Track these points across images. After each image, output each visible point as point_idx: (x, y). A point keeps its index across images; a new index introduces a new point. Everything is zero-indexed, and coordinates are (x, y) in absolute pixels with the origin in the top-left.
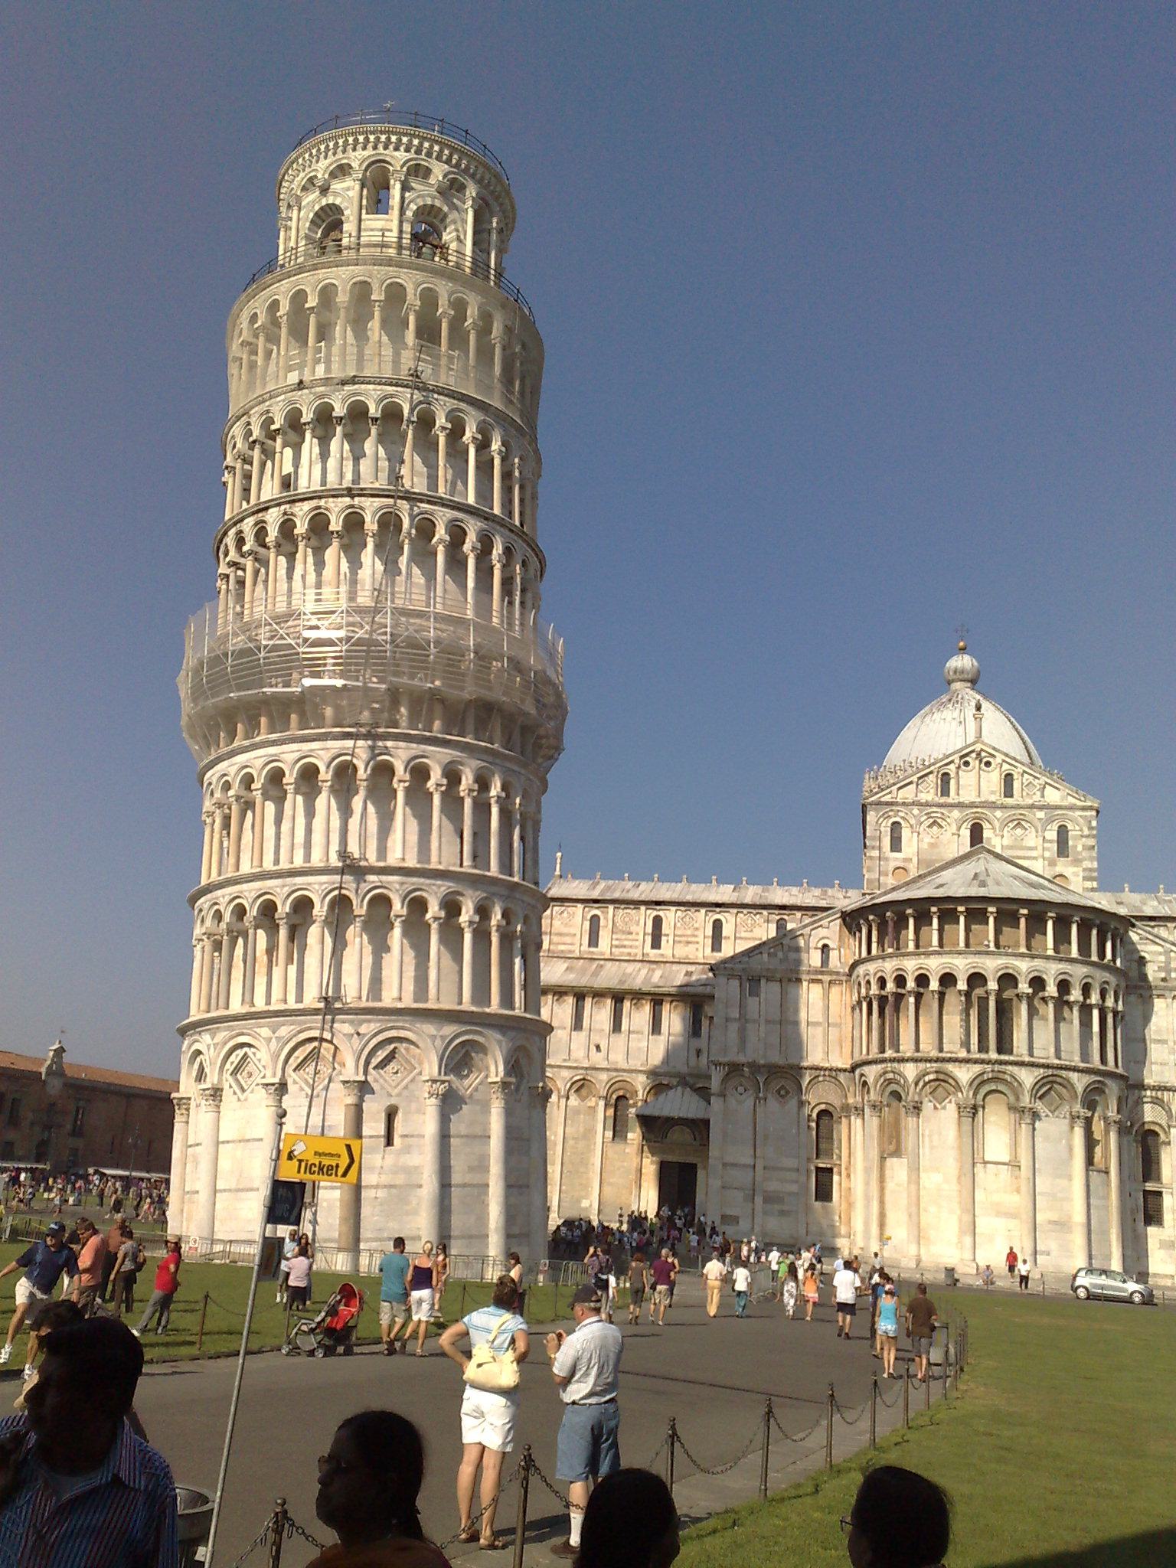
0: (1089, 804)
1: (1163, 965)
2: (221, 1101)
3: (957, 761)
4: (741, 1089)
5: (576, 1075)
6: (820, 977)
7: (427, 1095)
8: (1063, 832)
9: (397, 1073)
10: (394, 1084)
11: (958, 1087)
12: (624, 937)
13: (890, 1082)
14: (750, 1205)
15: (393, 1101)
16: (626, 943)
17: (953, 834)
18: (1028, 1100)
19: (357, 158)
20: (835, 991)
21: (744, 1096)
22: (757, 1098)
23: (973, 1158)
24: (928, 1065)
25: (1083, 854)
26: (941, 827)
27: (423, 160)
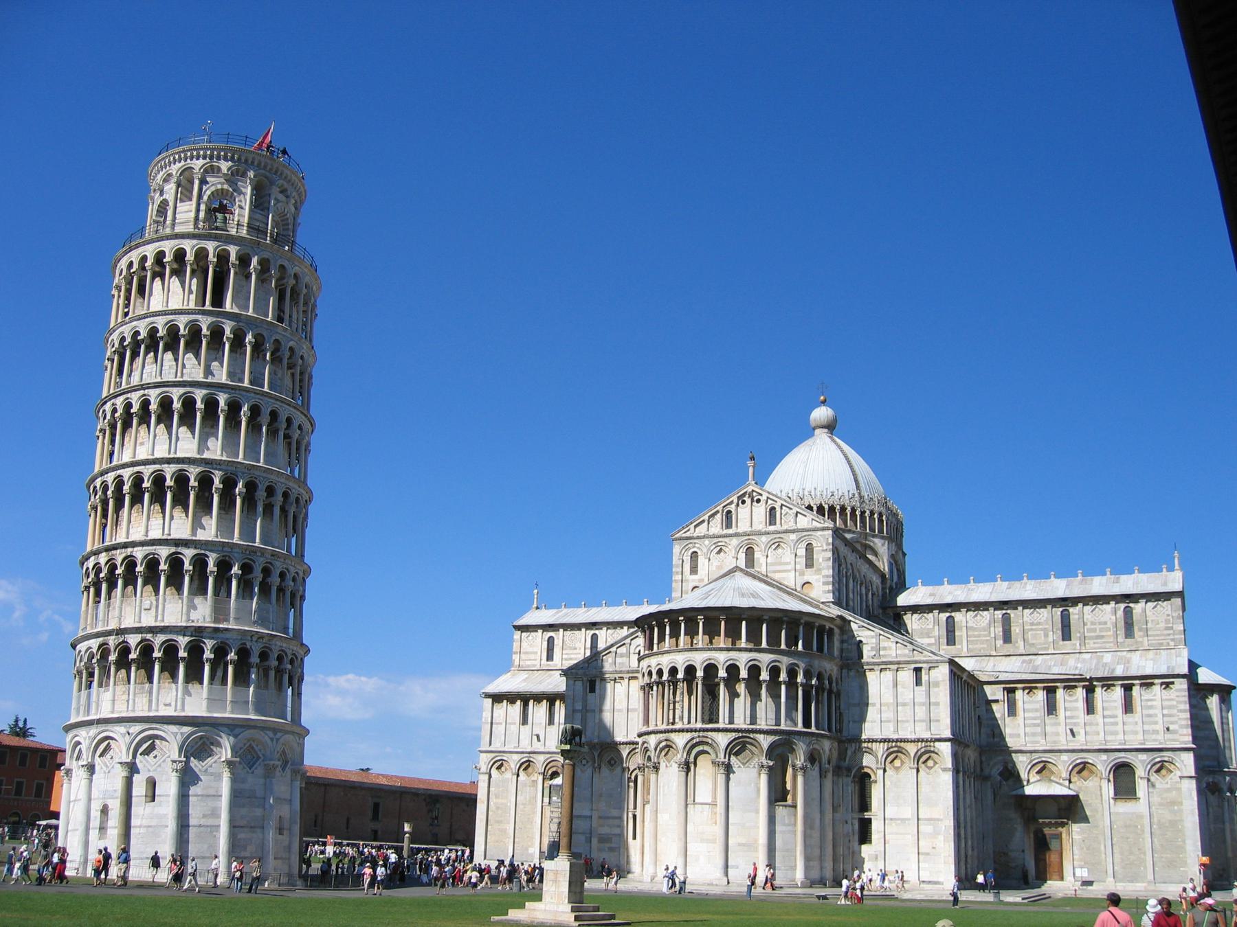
0: (826, 525)
1: (874, 645)
3: (736, 501)
4: (584, 762)
5: (523, 758)
8: (809, 549)
11: (677, 751)
12: (571, 652)
14: (589, 844)
16: (573, 656)
18: (722, 756)
19: (175, 169)
21: (585, 768)
23: (688, 799)
24: (661, 735)
25: (823, 565)
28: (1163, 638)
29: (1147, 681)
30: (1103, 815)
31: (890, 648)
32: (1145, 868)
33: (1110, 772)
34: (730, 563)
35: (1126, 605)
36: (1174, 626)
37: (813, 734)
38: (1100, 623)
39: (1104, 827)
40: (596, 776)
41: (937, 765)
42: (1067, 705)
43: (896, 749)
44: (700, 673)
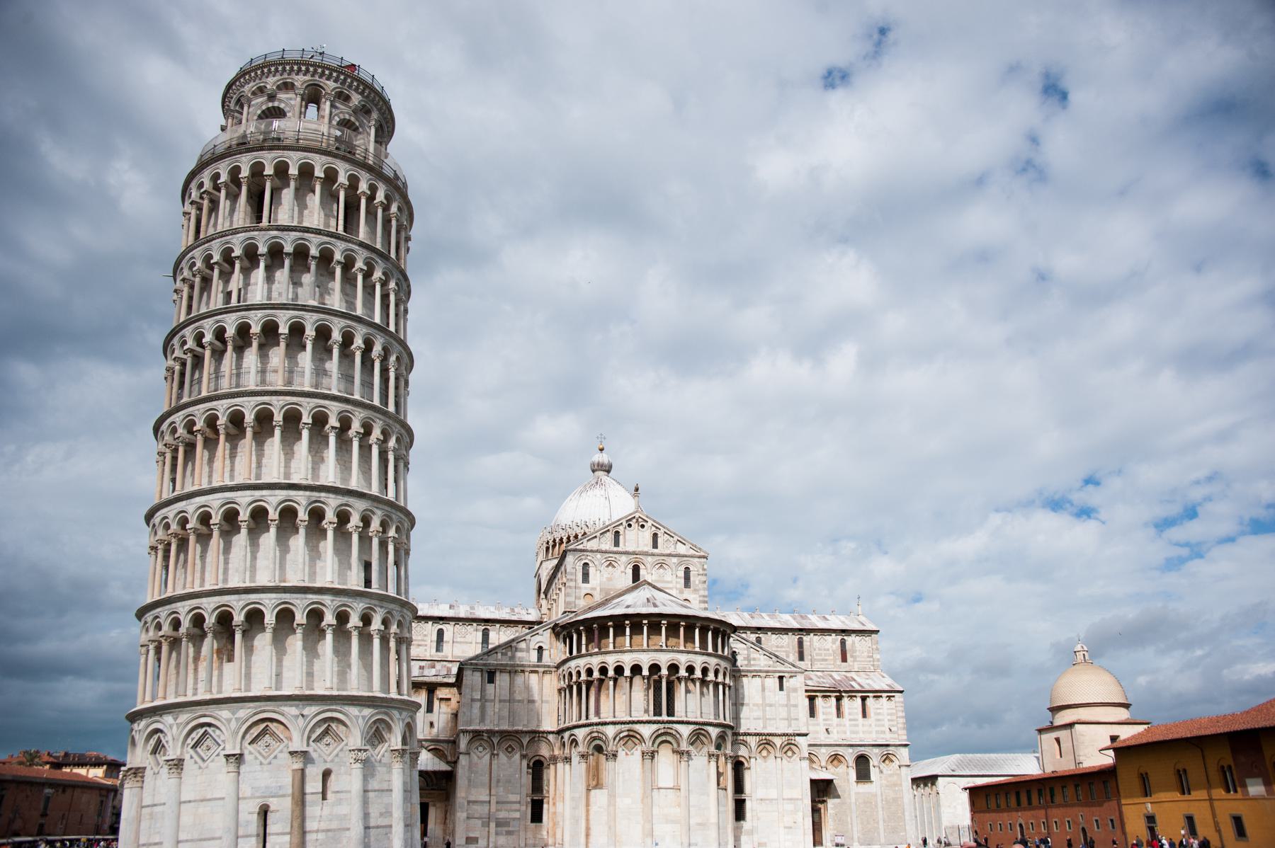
2: (182, 769)
3: (624, 524)
4: (481, 749)
6: (537, 669)
7: (352, 761)
8: (687, 570)
9: (329, 744)
10: (328, 753)
11: (642, 740)
13: (595, 739)
15: (328, 766)
17: (622, 572)
20: (547, 677)
22: (493, 754)
23: (652, 786)
24: (623, 726)
25: (700, 586)
26: (614, 567)
27: (346, 89)
29: (877, 694)
30: (850, 794)
31: (759, 659)
32: (878, 833)
35: (842, 637)
38: (825, 650)
39: (850, 803)
40: (495, 762)
41: (796, 755)
42: (825, 710)
43: (765, 742)
44: (664, 672)
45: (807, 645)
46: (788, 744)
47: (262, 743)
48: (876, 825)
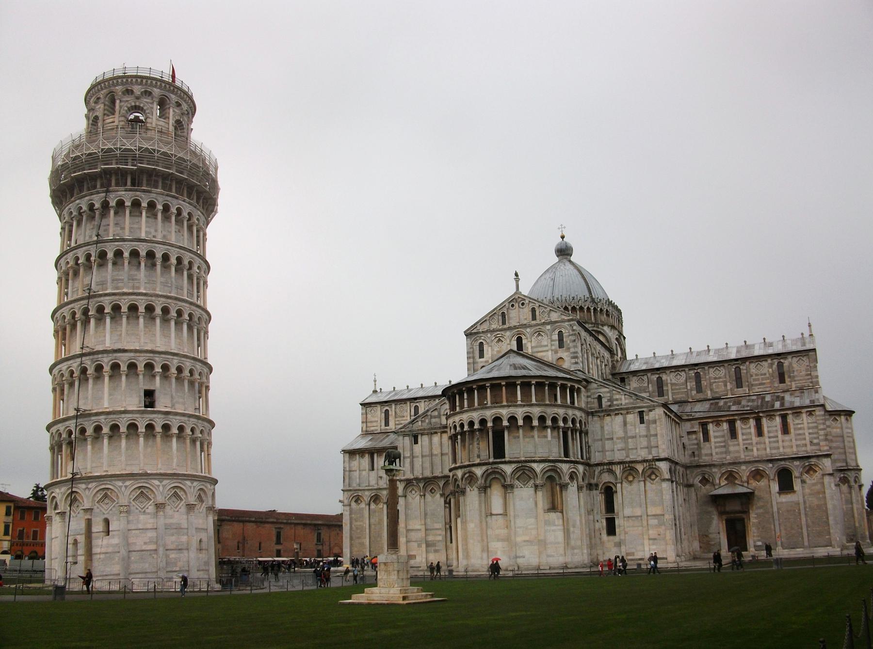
3: (507, 305)
4: (413, 492)
10: (106, 509)
11: (477, 479)
15: (106, 516)
16: (402, 422)
17: (508, 344)
19: (102, 94)
28: (804, 381)
29: (797, 411)
30: (772, 504)
31: (621, 399)
32: (803, 538)
33: (775, 475)
34: (505, 347)
36: (812, 373)
37: (571, 462)
38: (762, 375)
42: (744, 431)
43: (629, 468)
44: (490, 424)
45: (743, 373)
46: (650, 468)
47: (75, 505)
48: (800, 530)
